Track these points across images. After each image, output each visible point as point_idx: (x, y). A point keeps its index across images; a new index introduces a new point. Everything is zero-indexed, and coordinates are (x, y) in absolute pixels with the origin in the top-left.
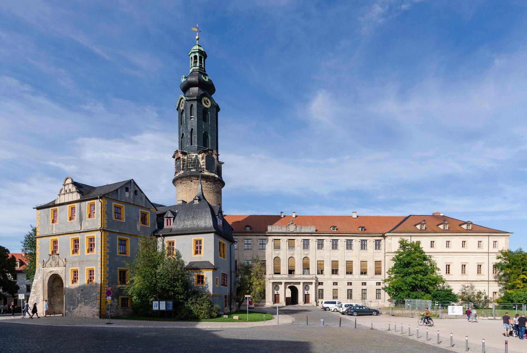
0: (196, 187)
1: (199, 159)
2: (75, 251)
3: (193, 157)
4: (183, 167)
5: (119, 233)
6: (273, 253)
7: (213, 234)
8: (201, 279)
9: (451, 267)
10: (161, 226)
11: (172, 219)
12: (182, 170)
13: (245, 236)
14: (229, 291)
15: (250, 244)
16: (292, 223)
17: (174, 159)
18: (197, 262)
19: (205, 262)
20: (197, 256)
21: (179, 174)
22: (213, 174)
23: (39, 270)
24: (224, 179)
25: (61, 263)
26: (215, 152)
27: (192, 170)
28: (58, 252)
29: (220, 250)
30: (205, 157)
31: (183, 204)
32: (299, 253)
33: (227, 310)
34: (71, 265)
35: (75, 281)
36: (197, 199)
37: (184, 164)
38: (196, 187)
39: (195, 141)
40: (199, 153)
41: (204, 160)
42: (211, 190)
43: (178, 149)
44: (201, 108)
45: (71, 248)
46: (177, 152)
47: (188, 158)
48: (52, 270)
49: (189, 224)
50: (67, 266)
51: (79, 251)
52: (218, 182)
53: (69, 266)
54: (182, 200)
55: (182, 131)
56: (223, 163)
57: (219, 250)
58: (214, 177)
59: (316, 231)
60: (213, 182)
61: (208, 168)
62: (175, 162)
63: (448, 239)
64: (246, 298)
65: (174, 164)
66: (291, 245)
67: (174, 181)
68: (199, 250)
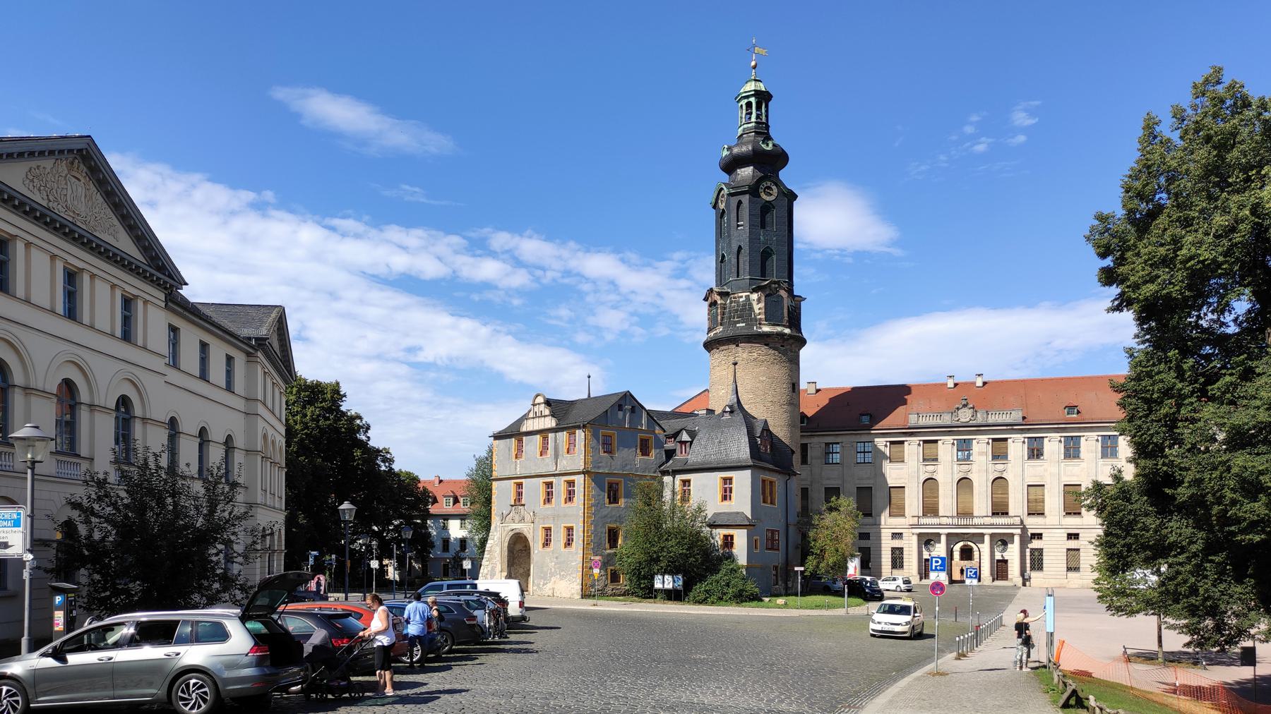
0: (745, 355)
1: (753, 302)
2: (548, 500)
3: (741, 300)
4: (722, 319)
7: (750, 471)
8: (728, 541)
11: (688, 444)
12: (721, 325)
13: (858, 436)
14: (785, 556)
15: (860, 452)
18: (724, 513)
19: (738, 513)
20: (726, 503)
21: (715, 332)
22: (779, 329)
23: (496, 527)
24: (805, 334)
25: (528, 518)
27: (738, 325)
28: (523, 502)
29: (764, 493)
30: (763, 298)
31: (708, 416)
33: (780, 587)
34: (541, 521)
35: (547, 545)
36: (727, 412)
37: (724, 314)
38: (745, 355)
39: (744, 269)
40: (754, 291)
41: (762, 305)
43: (713, 285)
45: (542, 496)
46: (712, 292)
47: (731, 302)
48: (514, 527)
50: (536, 521)
51: (553, 500)
52: (791, 341)
53: (539, 522)
54: (707, 409)
55: (723, 249)
57: (762, 493)
58: (781, 335)
61: (771, 318)
62: (709, 310)
64: (797, 571)
65: (706, 312)
67: (710, 345)
68: (728, 494)
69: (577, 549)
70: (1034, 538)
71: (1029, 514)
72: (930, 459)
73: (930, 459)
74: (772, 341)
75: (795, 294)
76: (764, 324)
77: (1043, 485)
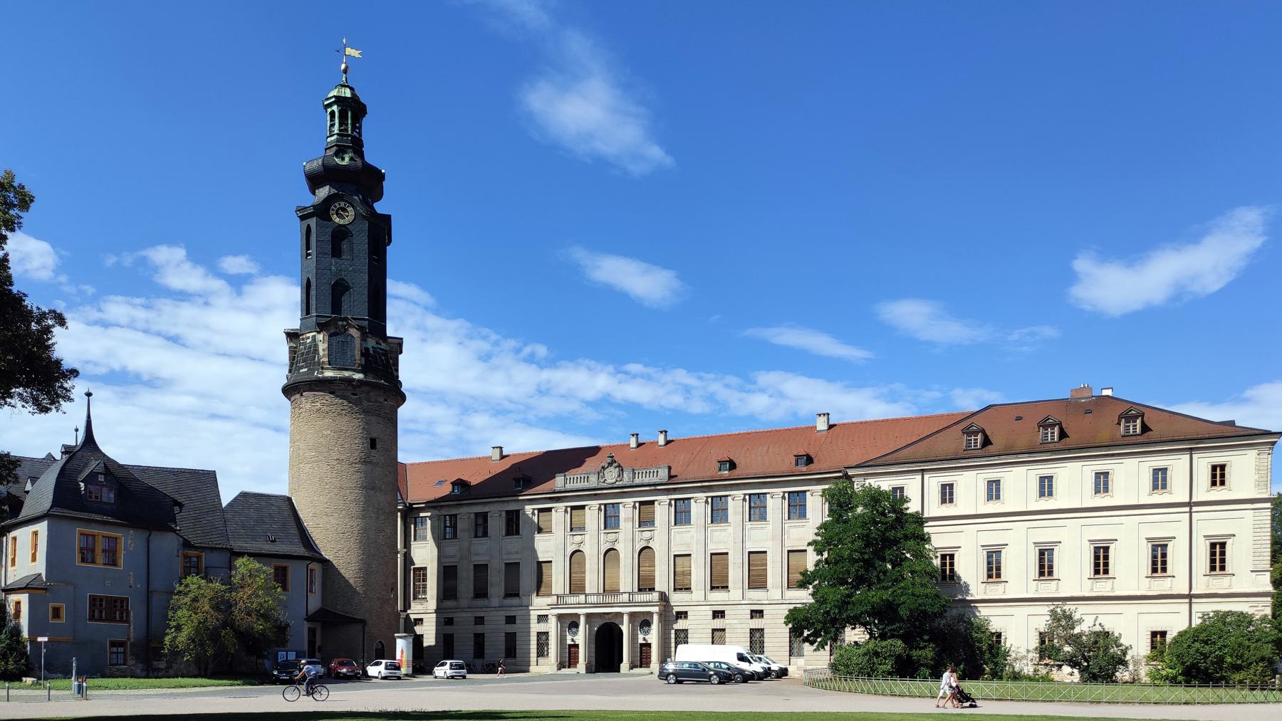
0: (308, 406)
6: (602, 538)
9: (1169, 550)
16: (609, 463)
22: (347, 374)
27: (301, 371)
30: (327, 338)
32: (627, 538)
38: (308, 406)
41: (326, 345)
42: (342, 410)
44: (327, 230)
52: (366, 389)
58: (349, 381)
59: (671, 477)
60: (349, 390)
63: (1045, 470)
66: (610, 521)
70: (681, 618)
71: (675, 590)
72: (576, 528)
73: (576, 528)
74: (337, 388)
75: (388, 335)
76: (327, 369)
77: (690, 555)
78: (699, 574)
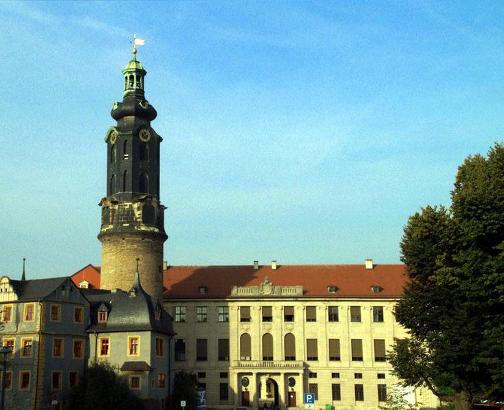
0: (129, 247)
3: (126, 207)
4: (113, 219)
5: (55, 335)
10: (94, 320)
11: (106, 313)
12: (112, 224)
17: (101, 207)
19: (141, 362)
22: (152, 229)
26: (154, 199)
27: (124, 225)
30: (141, 208)
37: (113, 216)
47: (119, 208)
49: (125, 320)
56: (166, 208)
69: (31, 388)
78: (323, 351)
